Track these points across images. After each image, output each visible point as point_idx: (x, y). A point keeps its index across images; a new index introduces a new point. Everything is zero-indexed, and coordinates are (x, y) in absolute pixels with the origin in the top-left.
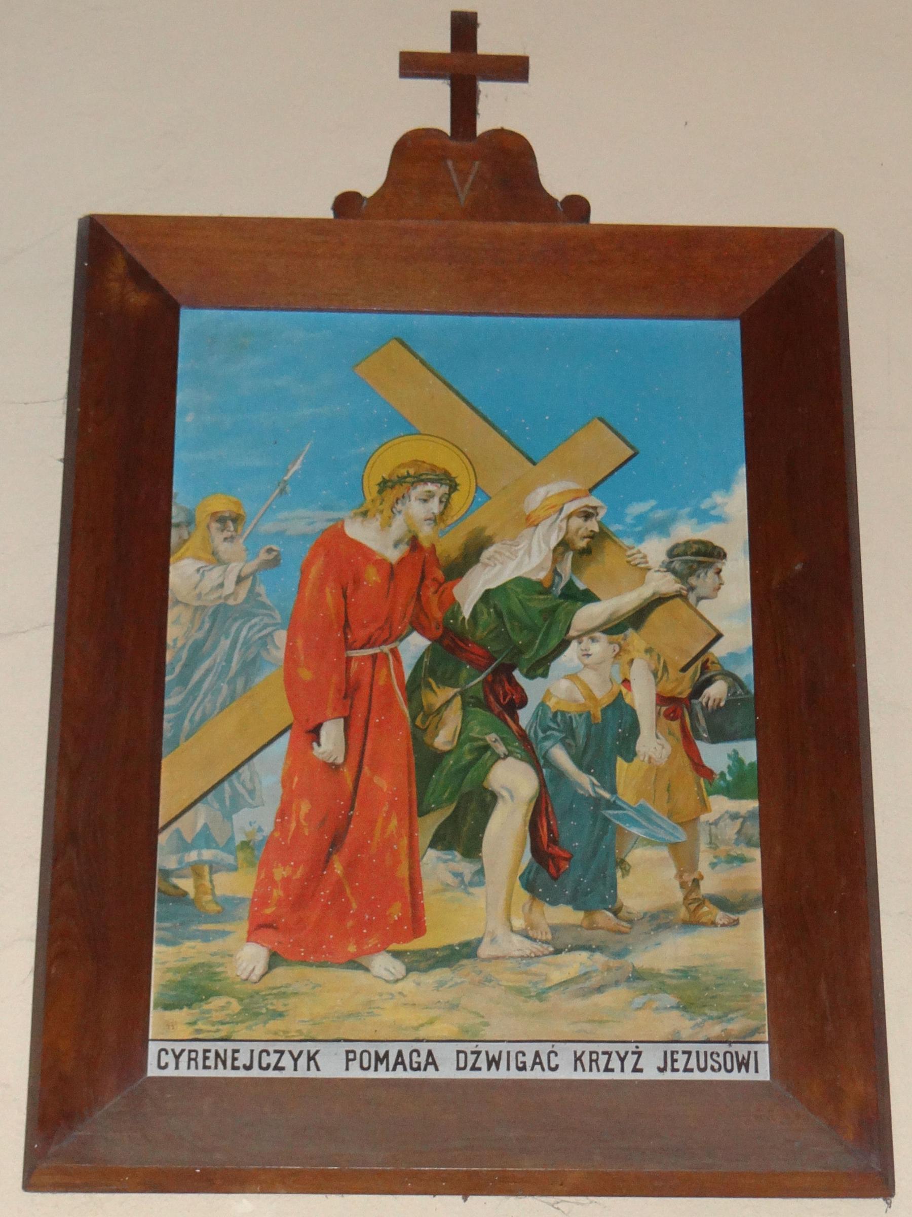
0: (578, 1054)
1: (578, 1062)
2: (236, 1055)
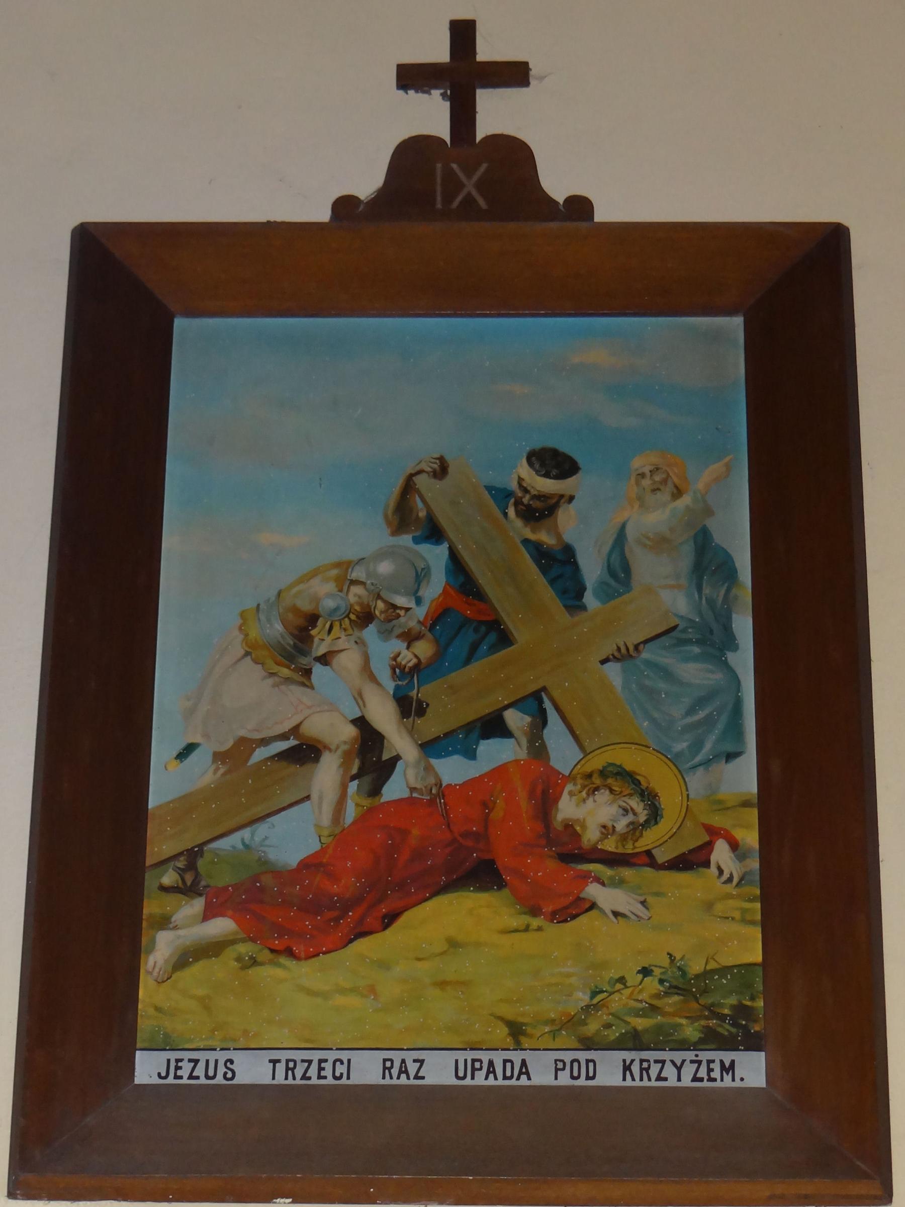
0: (628, 1063)
1: (628, 1073)
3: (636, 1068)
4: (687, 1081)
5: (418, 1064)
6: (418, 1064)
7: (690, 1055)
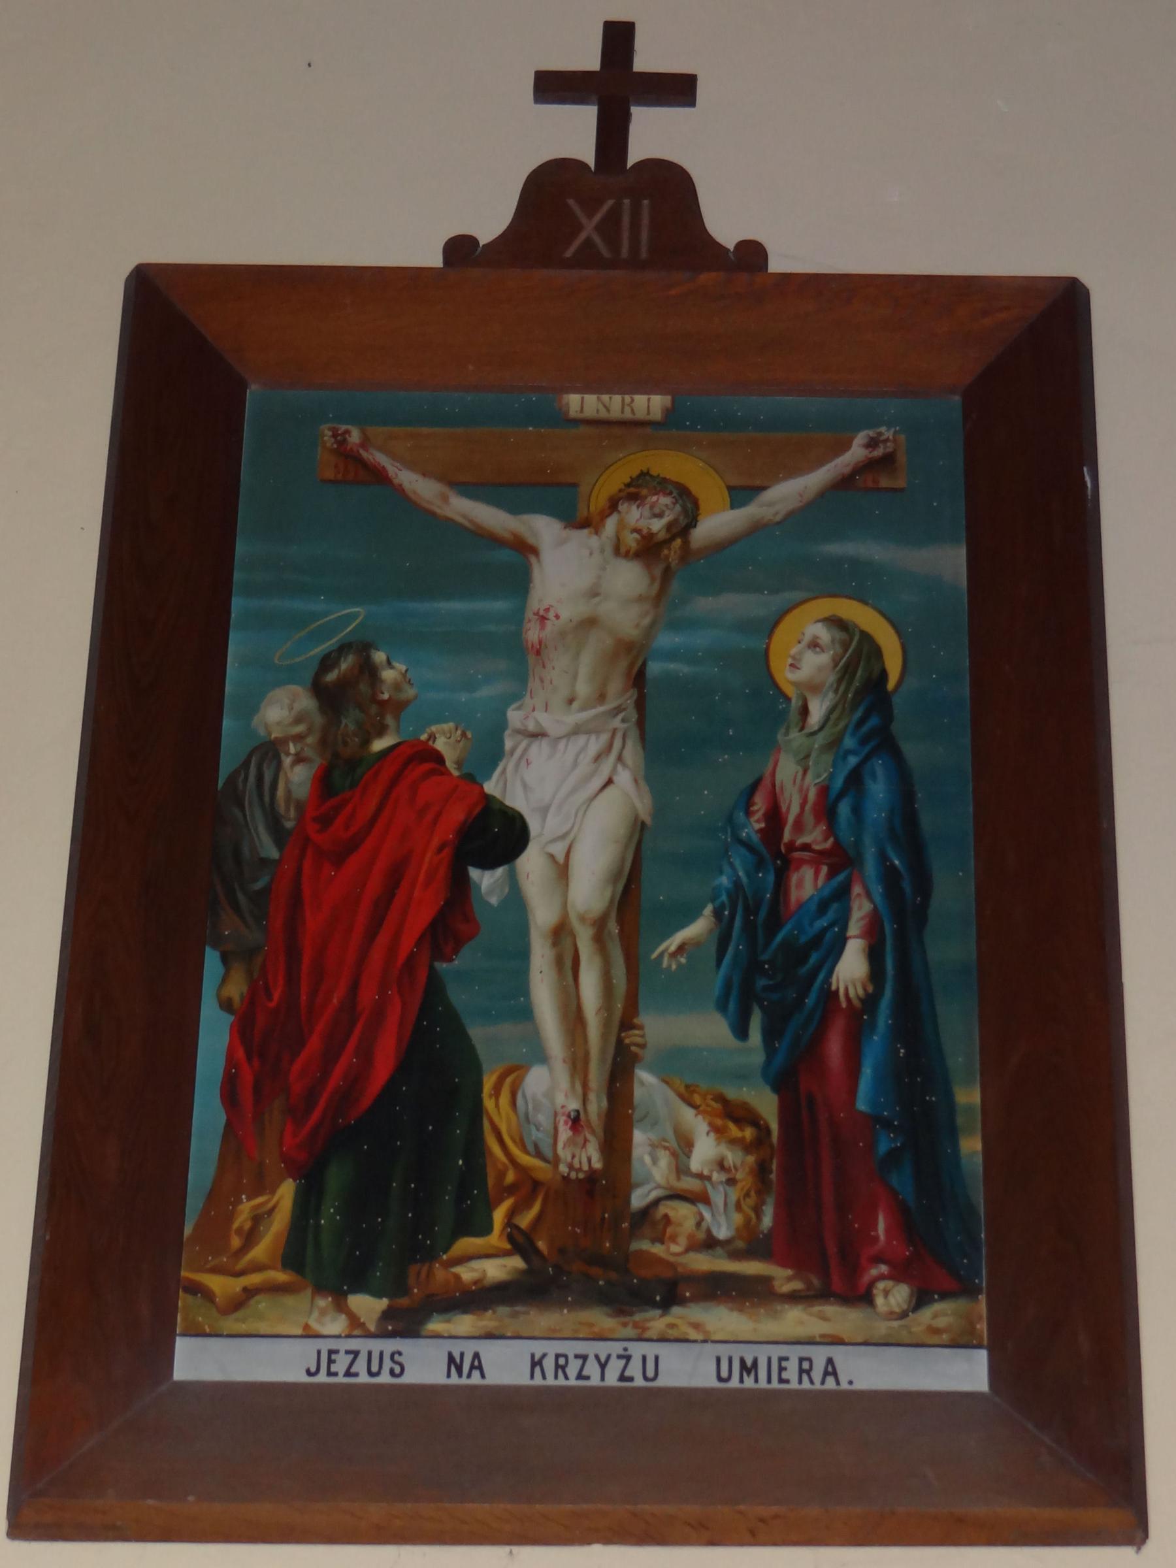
2: (784, 1364)
3: (549, 1364)
4: (612, 1379)
5: (351, 1357)
6: (351, 1357)
7: (616, 1348)
